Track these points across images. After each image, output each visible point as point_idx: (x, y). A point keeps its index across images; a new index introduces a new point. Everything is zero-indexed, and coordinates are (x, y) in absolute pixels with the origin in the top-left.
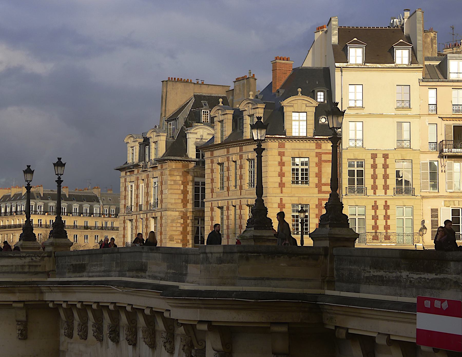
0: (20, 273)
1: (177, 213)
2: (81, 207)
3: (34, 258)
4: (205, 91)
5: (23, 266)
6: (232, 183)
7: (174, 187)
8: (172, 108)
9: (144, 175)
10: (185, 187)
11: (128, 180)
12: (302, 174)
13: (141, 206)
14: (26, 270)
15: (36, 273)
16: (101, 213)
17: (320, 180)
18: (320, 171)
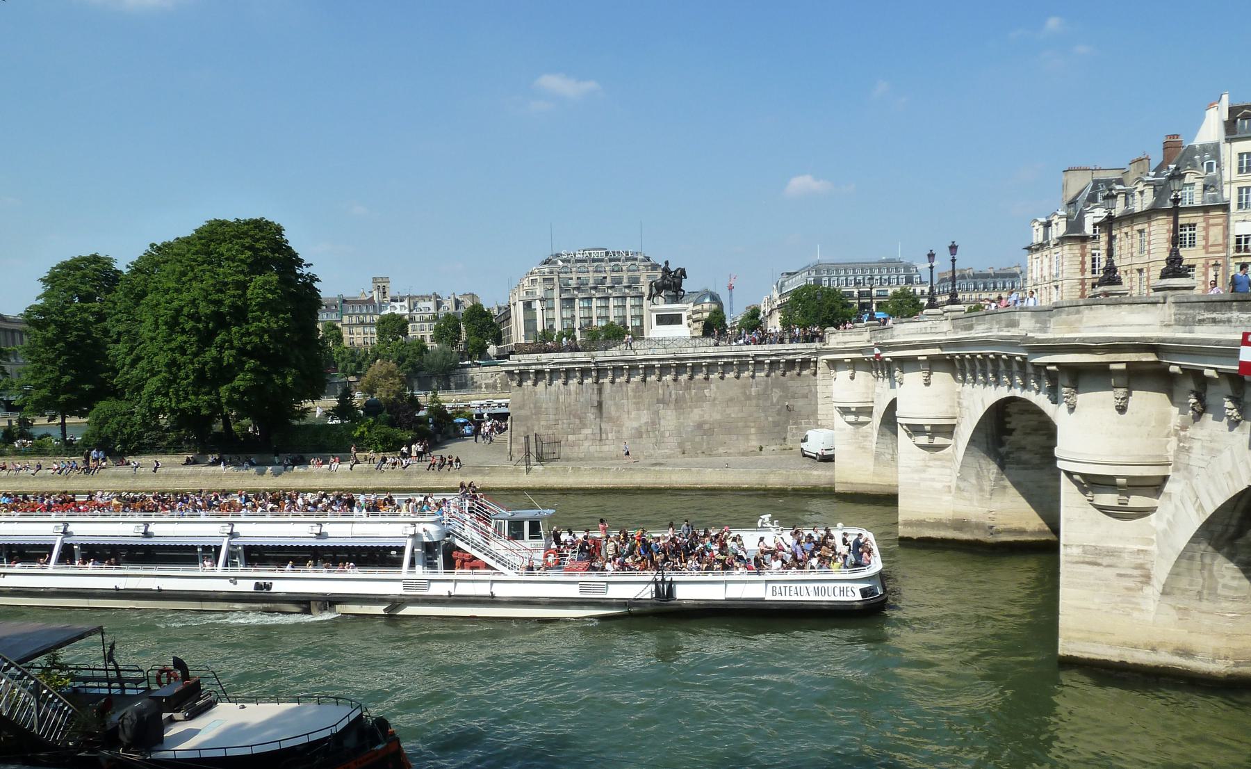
7: (1074, 259)
8: (1072, 193)
12: (1190, 239)
17: (1207, 243)
18: (1207, 234)
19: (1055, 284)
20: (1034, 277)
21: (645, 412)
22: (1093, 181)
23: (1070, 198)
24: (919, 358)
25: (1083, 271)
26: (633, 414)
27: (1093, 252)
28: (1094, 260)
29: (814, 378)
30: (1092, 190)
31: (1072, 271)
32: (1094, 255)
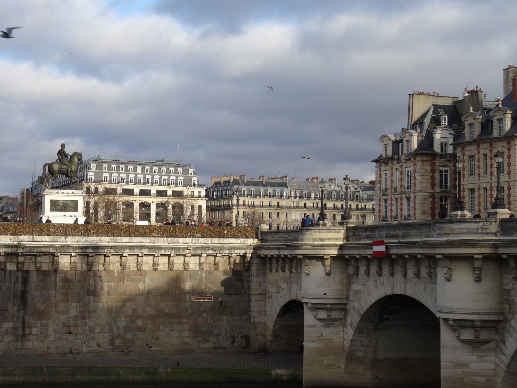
0: (475, 233)
1: (427, 194)
2: (274, 191)
3: (485, 223)
4: (440, 102)
5: (477, 229)
6: (482, 171)
7: (425, 174)
8: (417, 115)
9: (398, 166)
10: (433, 174)
11: (383, 169)
13: (396, 189)
14: (480, 231)
15: (487, 234)
16: (289, 195)
19: (385, 198)
20: (383, 187)
21: (74, 304)
22: (434, 105)
23: (415, 119)
24: (476, 256)
25: (433, 185)
26: (61, 307)
27: (441, 168)
28: (441, 176)
29: (246, 274)
30: (433, 113)
31: (424, 185)
32: (441, 171)
